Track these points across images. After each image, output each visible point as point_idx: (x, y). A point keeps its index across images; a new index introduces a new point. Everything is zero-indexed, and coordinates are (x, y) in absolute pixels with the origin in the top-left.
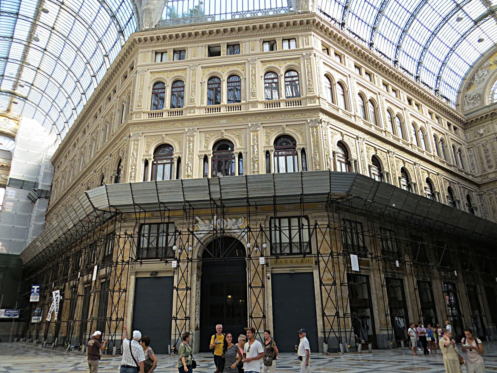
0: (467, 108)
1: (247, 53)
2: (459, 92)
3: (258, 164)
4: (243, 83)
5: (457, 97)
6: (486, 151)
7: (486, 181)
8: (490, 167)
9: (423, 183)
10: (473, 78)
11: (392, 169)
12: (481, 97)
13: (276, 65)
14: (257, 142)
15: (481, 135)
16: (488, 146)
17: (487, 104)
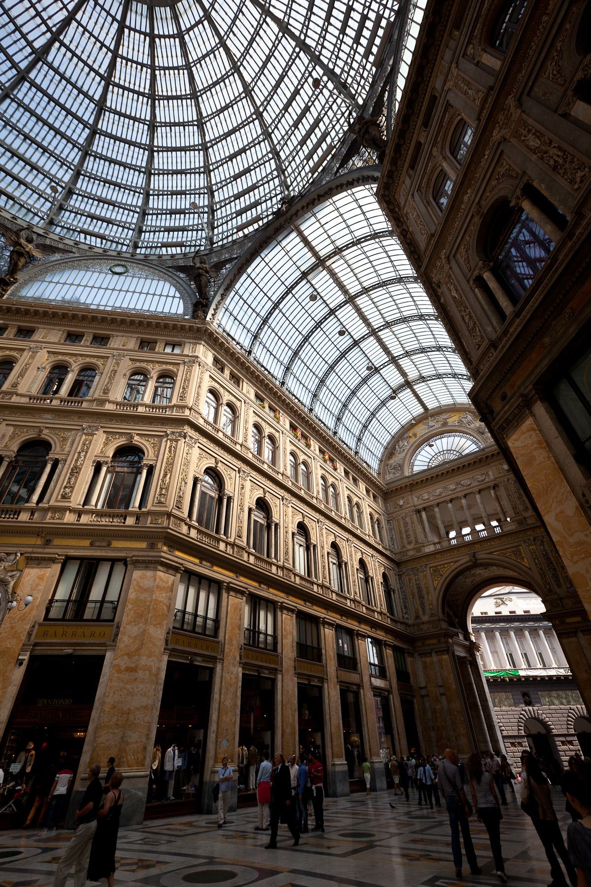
0: (388, 477)
1: (116, 346)
2: (381, 461)
3: (77, 478)
4: (97, 378)
5: (380, 465)
6: (406, 524)
7: (404, 558)
8: (410, 543)
9: (325, 546)
10: (394, 448)
11: (284, 521)
12: (400, 467)
13: (150, 367)
14: (88, 448)
15: (401, 506)
16: (408, 519)
17: (407, 474)
